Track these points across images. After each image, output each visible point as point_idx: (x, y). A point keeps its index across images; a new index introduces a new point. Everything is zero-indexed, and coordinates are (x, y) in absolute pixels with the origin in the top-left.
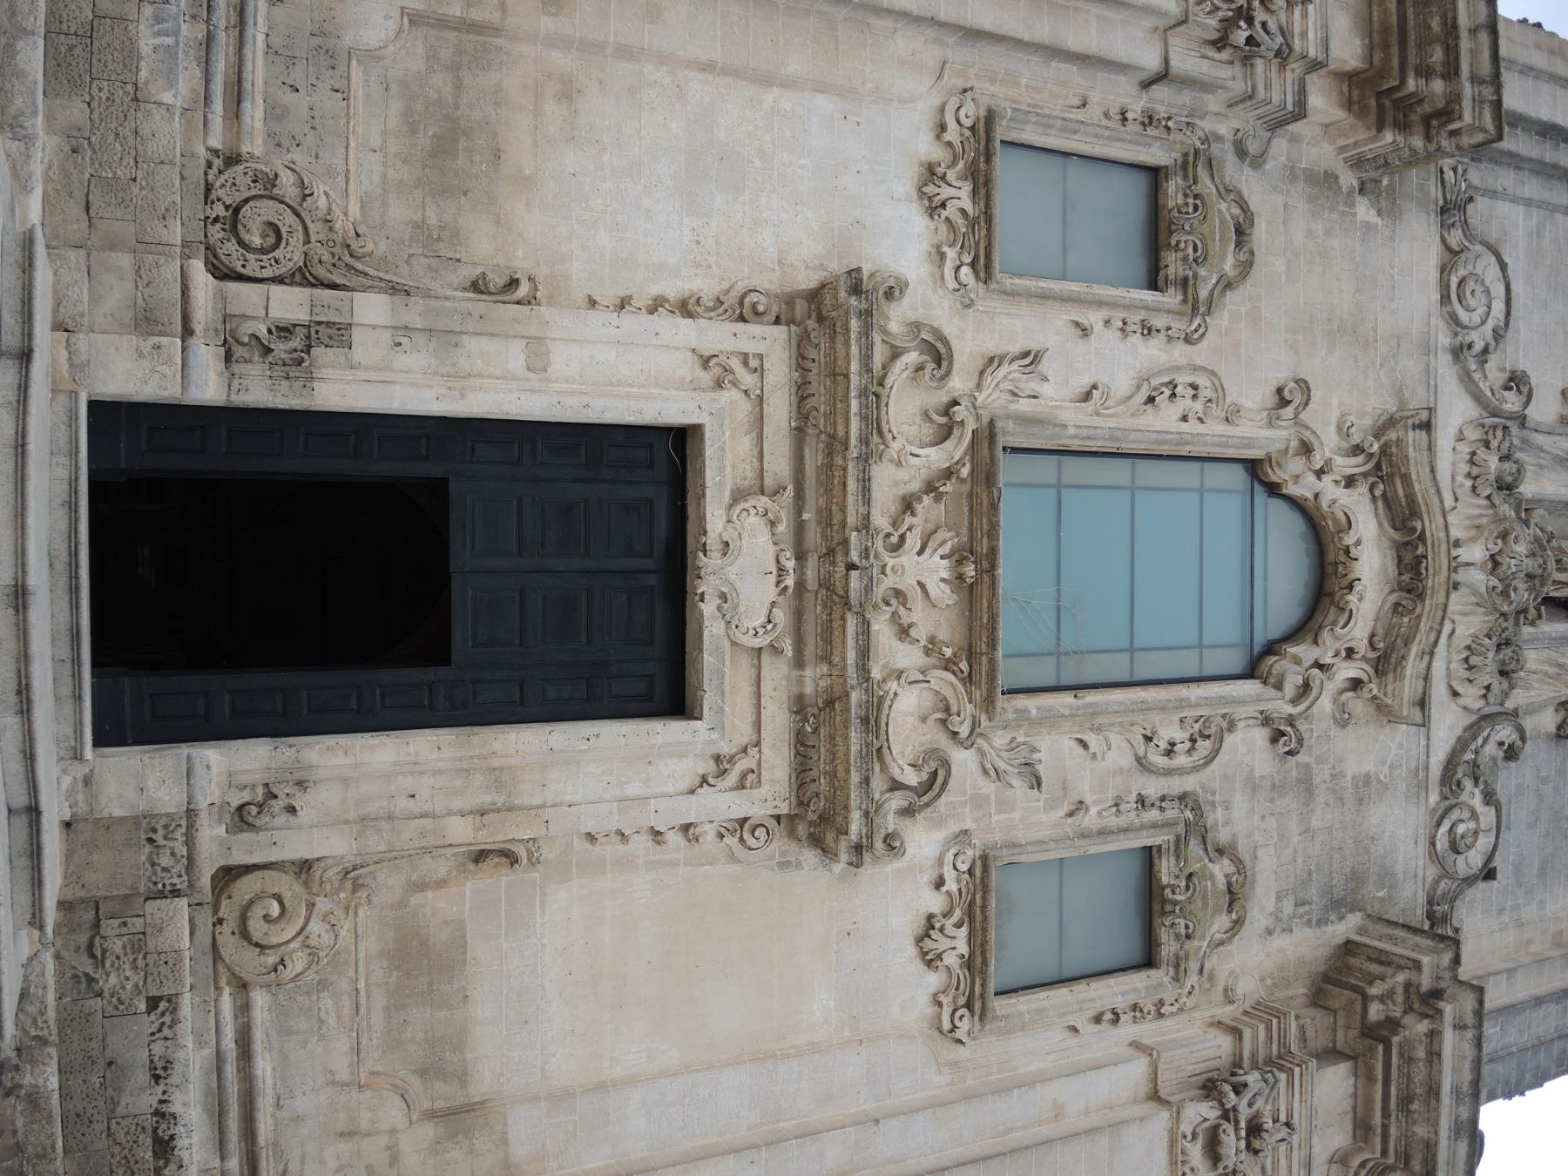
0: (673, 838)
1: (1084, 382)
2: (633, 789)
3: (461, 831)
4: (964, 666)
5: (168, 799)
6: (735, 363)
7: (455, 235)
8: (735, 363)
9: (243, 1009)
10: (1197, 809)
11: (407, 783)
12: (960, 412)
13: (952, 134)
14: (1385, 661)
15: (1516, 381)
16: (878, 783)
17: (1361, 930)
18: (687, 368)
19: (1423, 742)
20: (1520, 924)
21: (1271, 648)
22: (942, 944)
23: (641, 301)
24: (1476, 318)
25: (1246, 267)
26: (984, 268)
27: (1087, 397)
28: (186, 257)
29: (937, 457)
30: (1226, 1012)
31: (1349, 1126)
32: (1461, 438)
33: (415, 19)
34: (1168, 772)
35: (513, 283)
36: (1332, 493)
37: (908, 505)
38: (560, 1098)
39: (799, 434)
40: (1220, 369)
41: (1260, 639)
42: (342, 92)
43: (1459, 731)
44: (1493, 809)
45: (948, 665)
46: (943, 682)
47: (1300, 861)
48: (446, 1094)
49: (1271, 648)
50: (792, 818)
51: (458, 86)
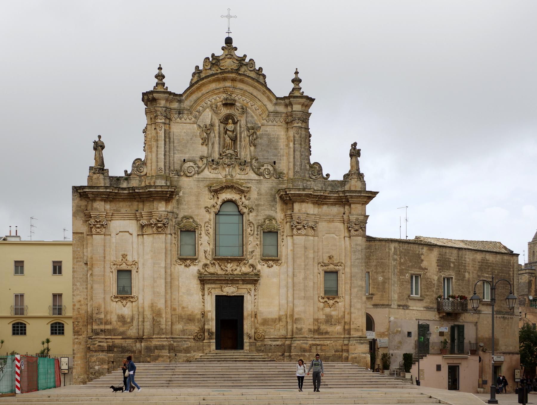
0: (256, 297)
1: (207, 244)
2: (250, 302)
3: (253, 319)
4: (240, 262)
5: (248, 344)
6: (209, 291)
7: (198, 319)
8: (209, 291)
9: (267, 338)
10: (259, 226)
11: (248, 324)
12: (212, 263)
13: (181, 263)
14: (241, 192)
15: (201, 158)
16: (252, 273)
17: (278, 195)
18: (210, 296)
19: (254, 181)
20: (283, 155)
21: (239, 212)
22: (270, 265)
23: (203, 300)
24: (193, 170)
25: (192, 218)
26: (196, 259)
27: (209, 244)
28: (203, 342)
29: (217, 266)
30: (285, 221)
31: (302, 203)
32: (211, 172)
33: (179, 323)
34: (254, 231)
35: (203, 314)
36: (219, 203)
37: (222, 269)
38: (280, 309)
39: (216, 283)
40: (204, 221)
41: (238, 213)
42: (187, 329)
43: (252, 172)
44: (265, 165)
45: (240, 264)
46: (241, 265)
47: (268, 206)
48: (277, 321)
49: (239, 212)
50: (255, 284)
51: (184, 319)
